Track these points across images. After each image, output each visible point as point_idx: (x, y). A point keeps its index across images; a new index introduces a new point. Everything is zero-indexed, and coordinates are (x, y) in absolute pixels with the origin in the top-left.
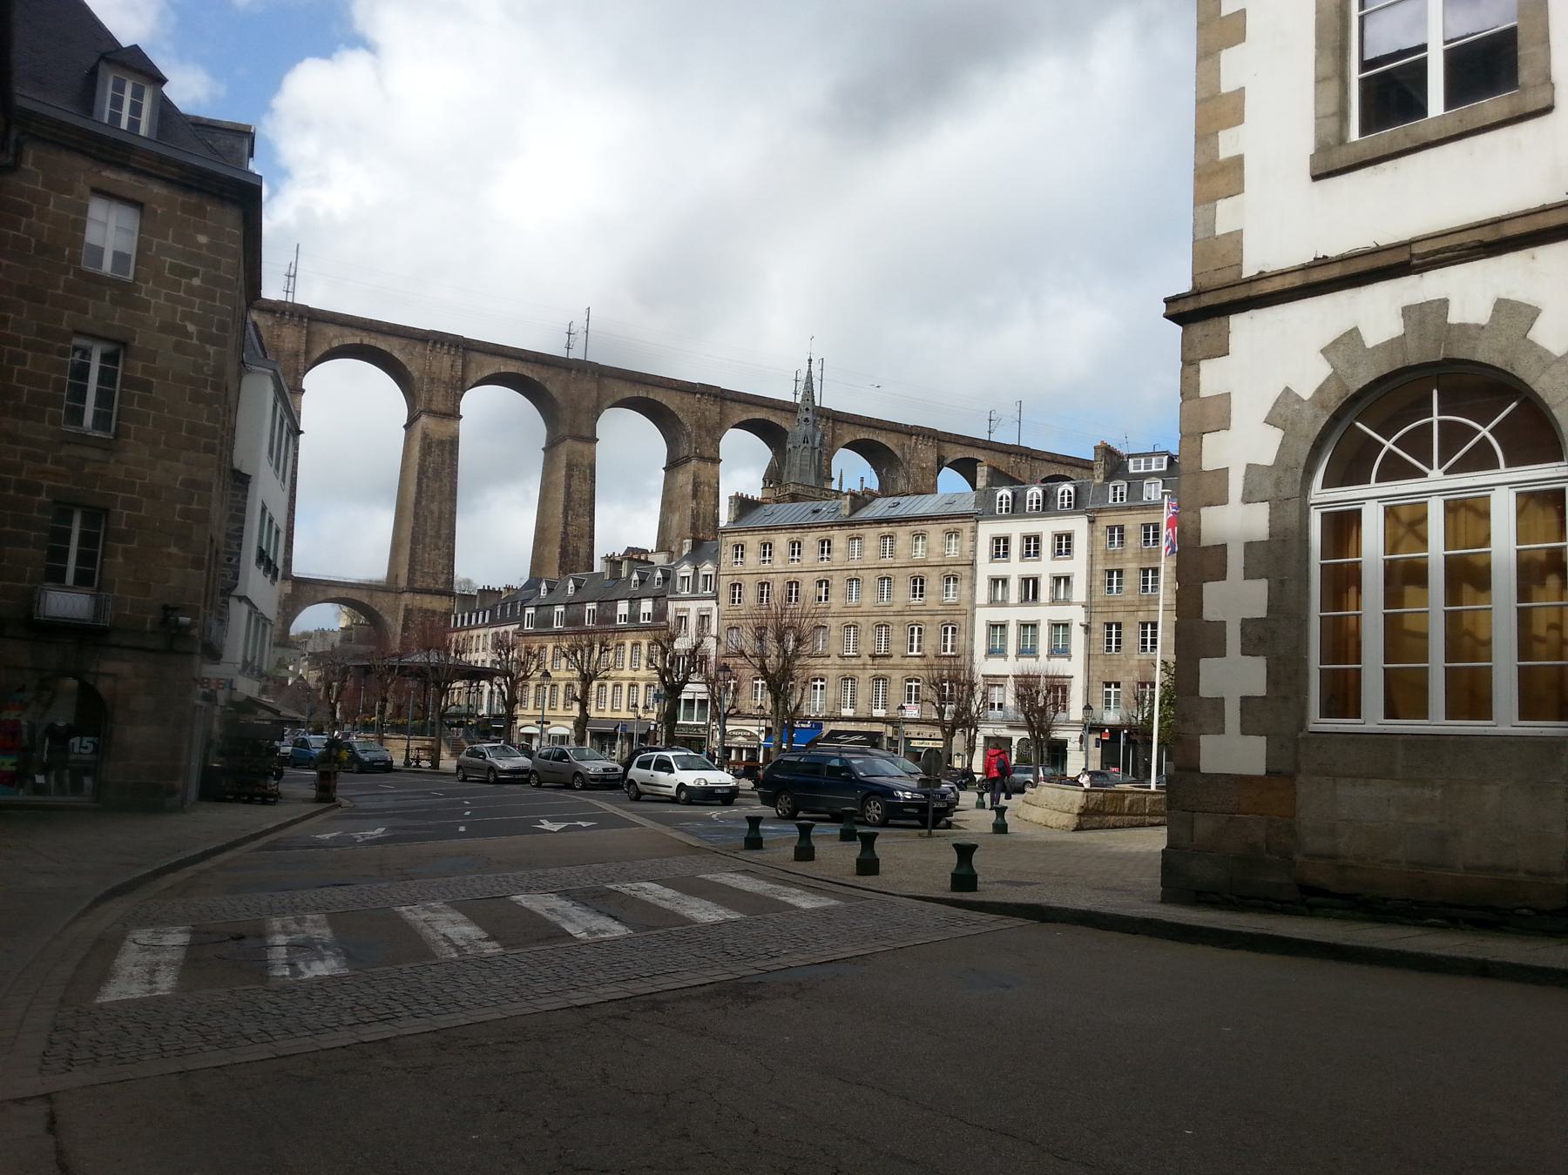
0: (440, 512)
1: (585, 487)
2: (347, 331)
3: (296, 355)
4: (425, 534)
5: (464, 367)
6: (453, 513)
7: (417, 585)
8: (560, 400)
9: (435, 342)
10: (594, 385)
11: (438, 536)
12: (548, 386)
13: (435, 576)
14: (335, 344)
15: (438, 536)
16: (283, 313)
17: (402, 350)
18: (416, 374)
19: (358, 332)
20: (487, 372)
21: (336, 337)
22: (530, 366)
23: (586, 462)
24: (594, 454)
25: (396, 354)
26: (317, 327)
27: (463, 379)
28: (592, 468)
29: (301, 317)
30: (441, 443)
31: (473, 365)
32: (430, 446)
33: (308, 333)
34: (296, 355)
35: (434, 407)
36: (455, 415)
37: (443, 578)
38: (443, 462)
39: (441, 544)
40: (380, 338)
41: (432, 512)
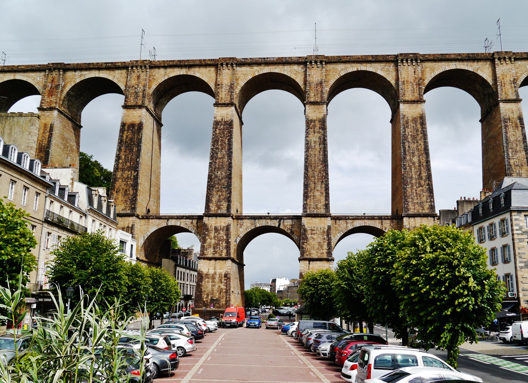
0: (420, 162)
1: (519, 133)
2: (348, 65)
3: (321, 83)
4: (411, 178)
5: (423, 72)
6: (428, 162)
7: (411, 212)
8: (490, 81)
9: (402, 61)
11: (420, 177)
12: (480, 73)
13: (421, 204)
14: (342, 74)
15: (420, 177)
16: (311, 62)
17: (382, 69)
18: (393, 82)
19: (354, 65)
20: (437, 73)
21: (342, 70)
22: (465, 63)
23: (516, 116)
25: (379, 72)
26: (330, 67)
27: (422, 79)
28: (521, 119)
29: (321, 62)
30: (414, 120)
31: (428, 69)
32: (407, 123)
33: (327, 70)
34: (321, 83)
35: (407, 99)
36: (420, 101)
37: (427, 206)
38: (417, 131)
39: (423, 182)
40: (369, 65)
41: (414, 163)
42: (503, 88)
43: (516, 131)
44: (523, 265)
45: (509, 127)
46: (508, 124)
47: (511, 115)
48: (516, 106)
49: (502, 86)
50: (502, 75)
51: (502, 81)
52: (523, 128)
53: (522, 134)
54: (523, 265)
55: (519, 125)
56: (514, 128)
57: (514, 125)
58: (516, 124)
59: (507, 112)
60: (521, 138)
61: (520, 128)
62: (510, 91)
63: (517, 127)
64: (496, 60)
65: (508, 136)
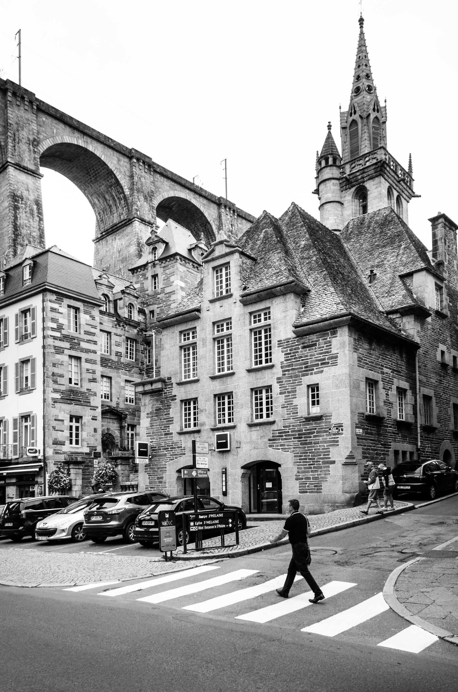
10: (30, 116)
24: (38, 189)
28: (38, 203)
42: (17, 145)
43: (31, 220)
44: (58, 396)
45: (21, 210)
46: (20, 205)
47: (25, 194)
48: (34, 183)
49: (14, 140)
50: (17, 123)
51: (17, 133)
52: (41, 220)
53: (39, 229)
54: (58, 396)
55: (36, 214)
56: (28, 215)
57: (28, 209)
58: (32, 210)
59: (19, 185)
60: (36, 234)
61: (38, 219)
62: (27, 154)
63: (32, 214)
64: (9, 94)
65: (18, 223)
